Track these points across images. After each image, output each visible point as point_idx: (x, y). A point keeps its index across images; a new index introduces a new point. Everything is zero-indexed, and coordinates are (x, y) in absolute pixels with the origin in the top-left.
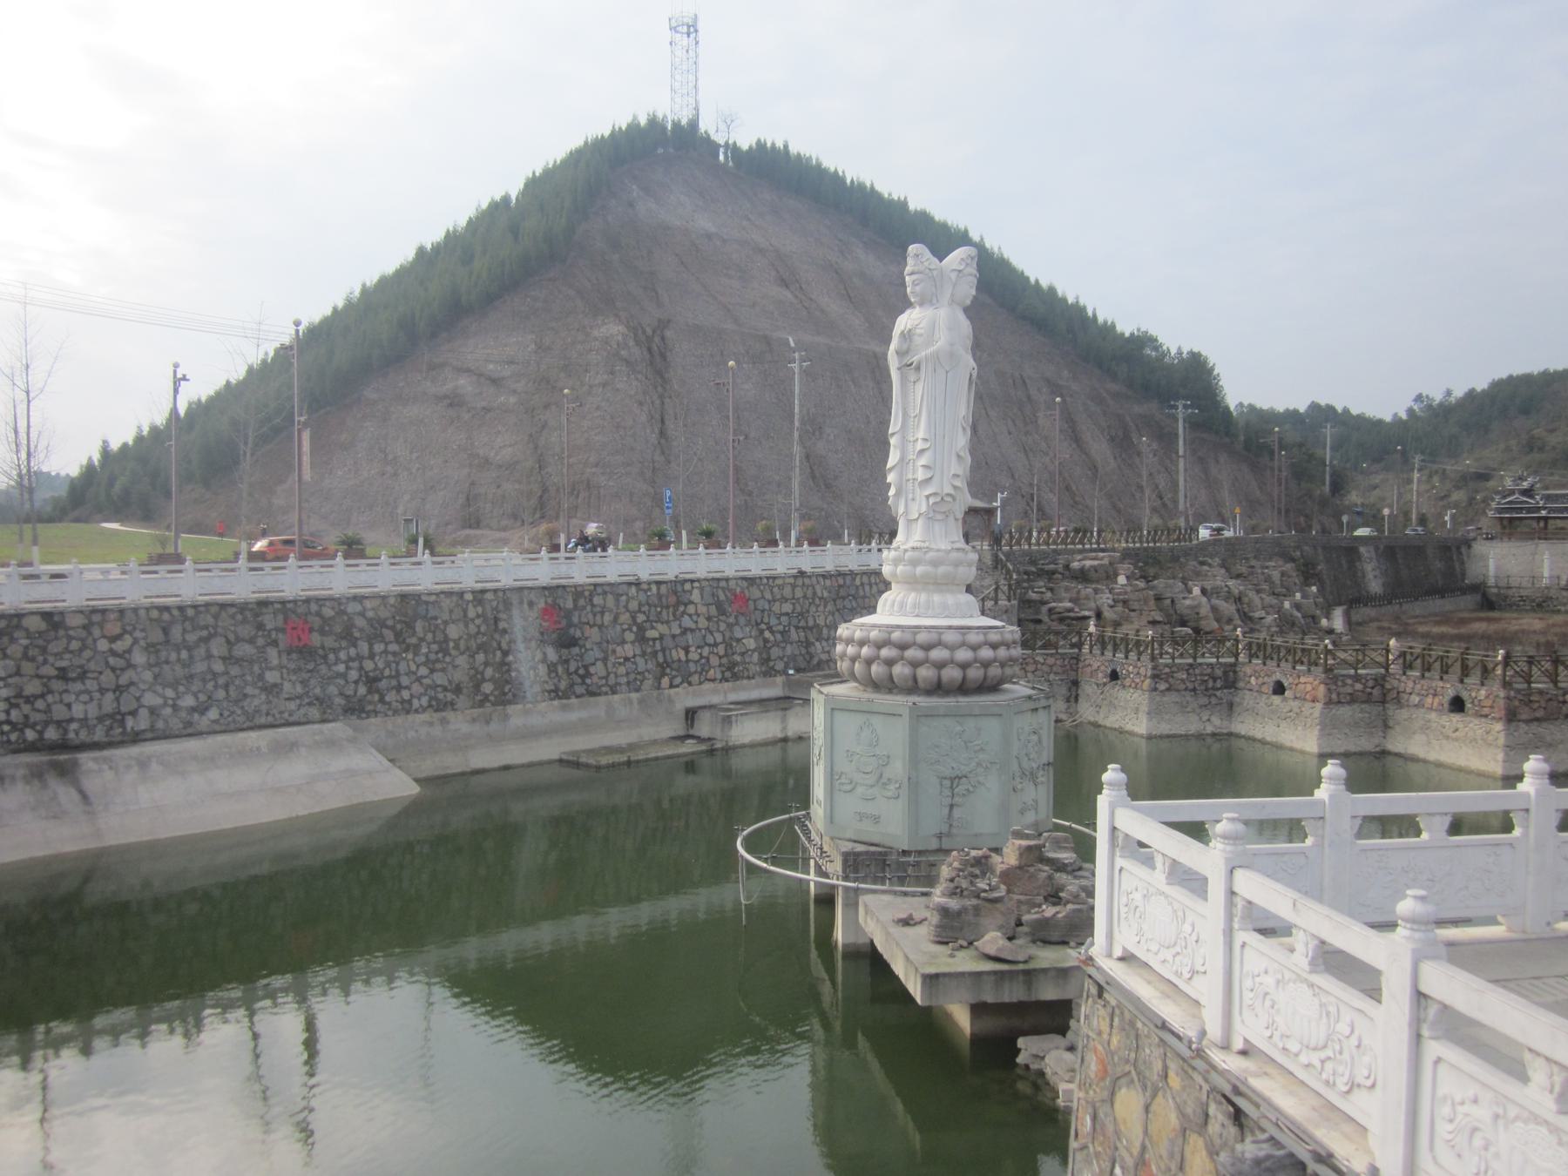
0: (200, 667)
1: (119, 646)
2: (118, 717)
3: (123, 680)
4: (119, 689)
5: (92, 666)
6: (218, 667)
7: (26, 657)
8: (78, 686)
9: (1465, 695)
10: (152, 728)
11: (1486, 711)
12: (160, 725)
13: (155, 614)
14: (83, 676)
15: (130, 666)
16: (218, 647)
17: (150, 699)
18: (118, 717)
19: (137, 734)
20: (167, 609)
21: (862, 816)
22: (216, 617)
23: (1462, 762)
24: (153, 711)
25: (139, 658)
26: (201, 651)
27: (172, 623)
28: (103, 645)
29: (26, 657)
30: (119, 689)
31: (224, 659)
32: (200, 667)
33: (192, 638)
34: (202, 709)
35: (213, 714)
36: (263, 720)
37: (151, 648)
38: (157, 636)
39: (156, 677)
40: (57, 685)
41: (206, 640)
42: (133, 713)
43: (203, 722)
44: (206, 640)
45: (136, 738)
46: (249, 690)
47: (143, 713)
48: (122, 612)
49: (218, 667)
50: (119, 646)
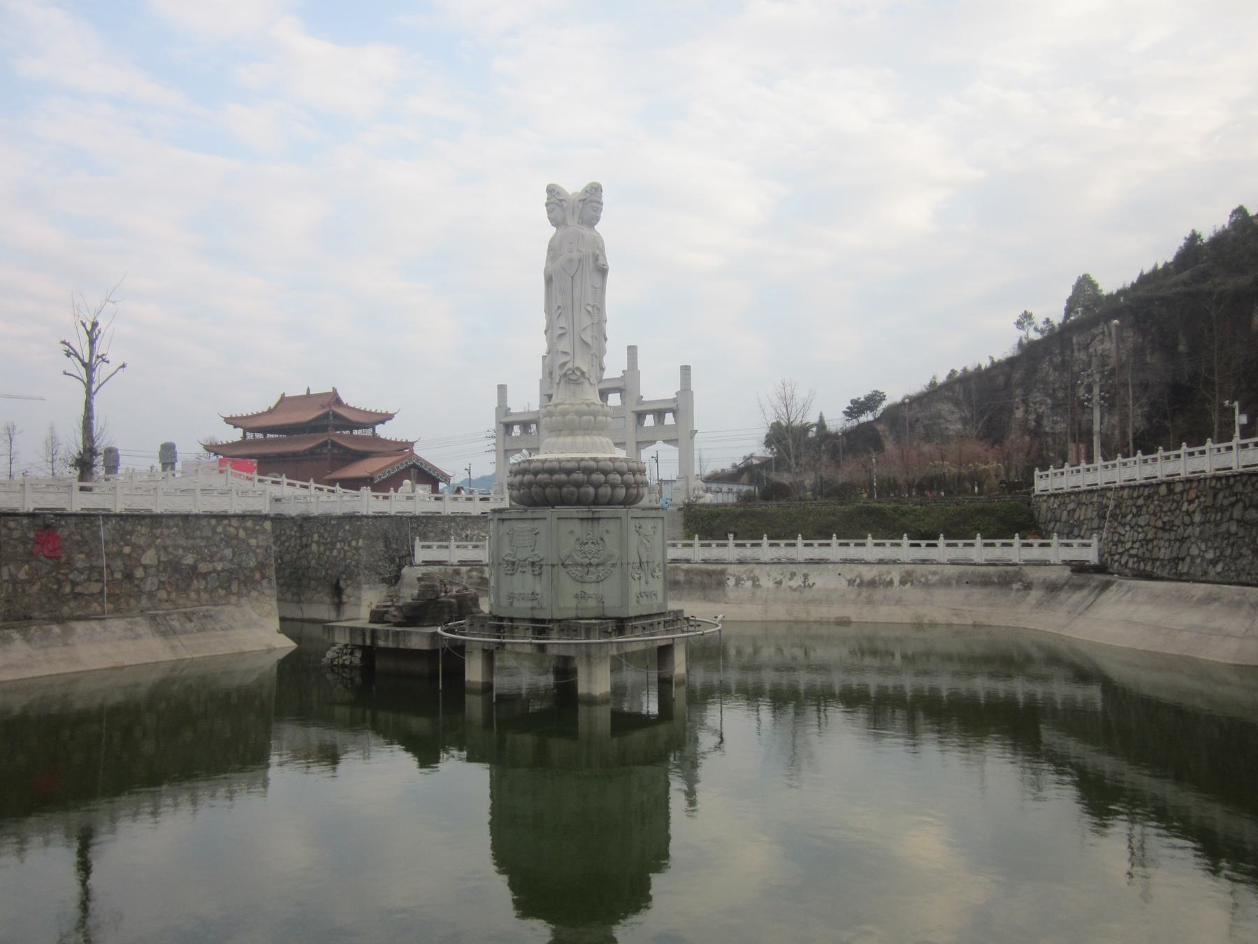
0: (1223, 528)
1: (1192, 507)
2: (1177, 560)
3: (1186, 535)
4: (1183, 540)
5: (1177, 522)
6: (1233, 528)
7: (1154, 514)
8: (1167, 536)
10: (1188, 573)
12: (1192, 571)
13: (1214, 483)
14: (1171, 530)
15: (1192, 523)
16: (1237, 513)
17: (1194, 551)
18: (1177, 560)
19: (1181, 574)
20: (1218, 478)
22: (1244, 485)
24: (1193, 558)
25: (1197, 518)
26: (1228, 514)
27: (1220, 490)
28: (1184, 508)
29: (1154, 514)
30: (1183, 540)
31: (1238, 521)
32: (1223, 528)
33: (1226, 502)
34: (1214, 562)
35: (1219, 568)
36: (1244, 578)
37: (1205, 511)
38: (1209, 502)
39: (1201, 532)
40: (1160, 534)
41: (1233, 505)
42: (1183, 559)
43: (1212, 572)
44: (1233, 505)
45: (1179, 578)
46: (1245, 551)
47: (1188, 559)
48: (1199, 480)
49: (1233, 528)
50: (1192, 507)
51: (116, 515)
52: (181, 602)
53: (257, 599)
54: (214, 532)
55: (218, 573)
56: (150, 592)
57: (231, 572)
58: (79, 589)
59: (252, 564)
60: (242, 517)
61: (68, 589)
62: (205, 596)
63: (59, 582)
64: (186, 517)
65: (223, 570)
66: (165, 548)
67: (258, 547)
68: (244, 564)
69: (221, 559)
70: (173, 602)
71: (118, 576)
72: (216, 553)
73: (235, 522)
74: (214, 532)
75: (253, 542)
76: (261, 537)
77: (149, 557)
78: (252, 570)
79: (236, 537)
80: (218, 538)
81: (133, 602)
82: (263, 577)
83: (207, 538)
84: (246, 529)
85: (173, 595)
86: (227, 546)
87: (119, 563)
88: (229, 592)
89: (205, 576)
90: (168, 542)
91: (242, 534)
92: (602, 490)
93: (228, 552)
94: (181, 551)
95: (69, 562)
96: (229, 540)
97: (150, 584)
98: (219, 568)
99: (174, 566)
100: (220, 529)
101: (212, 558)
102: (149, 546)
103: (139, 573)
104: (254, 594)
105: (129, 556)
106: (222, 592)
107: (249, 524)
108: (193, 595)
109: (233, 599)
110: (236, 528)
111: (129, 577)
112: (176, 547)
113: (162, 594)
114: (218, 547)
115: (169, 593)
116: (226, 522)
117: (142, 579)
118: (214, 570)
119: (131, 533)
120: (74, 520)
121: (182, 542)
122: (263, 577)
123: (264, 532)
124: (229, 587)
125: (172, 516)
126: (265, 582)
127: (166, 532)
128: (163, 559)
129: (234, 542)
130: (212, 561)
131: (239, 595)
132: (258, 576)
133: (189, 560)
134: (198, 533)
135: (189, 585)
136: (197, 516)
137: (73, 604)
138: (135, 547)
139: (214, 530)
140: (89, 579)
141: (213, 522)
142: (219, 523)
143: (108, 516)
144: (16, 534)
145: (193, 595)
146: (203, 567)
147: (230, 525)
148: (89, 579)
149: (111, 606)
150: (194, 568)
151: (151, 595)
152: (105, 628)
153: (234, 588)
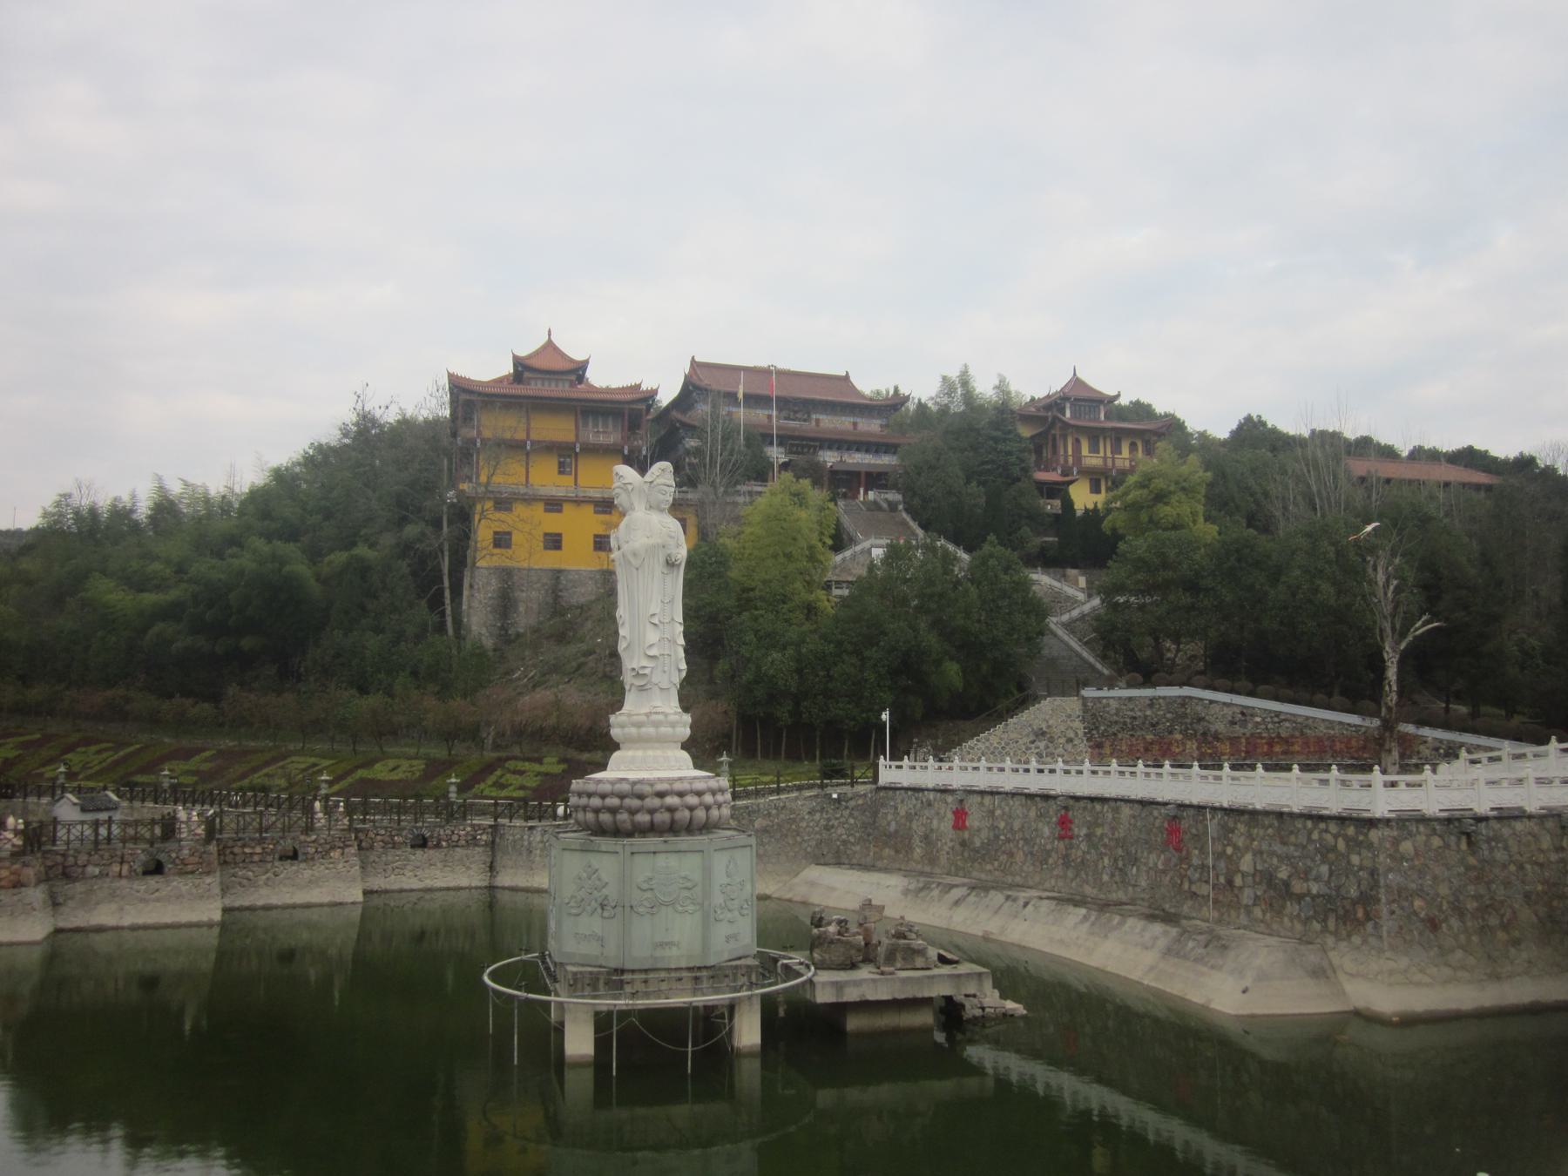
9: (162, 857)
11: (190, 868)
21: (728, 939)
23: (167, 919)
51: (1222, 809)
52: (1275, 926)
53: (1358, 948)
54: (1309, 839)
55: (1314, 898)
56: (1247, 906)
57: (1328, 898)
58: (1194, 888)
59: (1353, 892)
60: (1341, 820)
61: (1186, 886)
62: (1298, 927)
63: (1182, 877)
64: (1280, 815)
65: (1318, 895)
66: (1261, 853)
67: (1361, 868)
68: (1343, 892)
69: (1317, 879)
70: (1268, 926)
71: (1222, 880)
72: (1311, 869)
73: (1333, 828)
74: (1309, 839)
75: (1355, 859)
76: (1365, 852)
77: (1246, 863)
78: (1354, 903)
79: (1334, 849)
80: (1311, 847)
81: (1233, 914)
82: (1368, 917)
83: (1304, 847)
84: (1347, 839)
85: (1268, 915)
86: (1323, 862)
87: (1222, 864)
88: (1325, 929)
89: (1300, 898)
90: (1265, 847)
91: (1341, 845)
92: (678, 815)
93: (1324, 869)
94: (1275, 861)
95: (1188, 858)
96: (1326, 851)
97: (1247, 896)
98: (1314, 891)
99: (1268, 878)
100: (1315, 836)
101: (1305, 875)
102: (1247, 849)
103: (1238, 881)
104: (1356, 940)
105: (1229, 858)
106: (1317, 926)
107: (1351, 831)
108: (1286, 920)
109: (1330, 940)
110: (1336, 837)
111: (1230, 882)
112: (1273, 854)
113: (1258, 912)
114: (1313, 860)
115: (1264, 912)
116: (1322, 826)
117: (1241, 888)
118: (1309, 893)
119: (1232, 831)
120: (1192, 812)
121: (1278, 848)
122: (1368, 917)
123: (1370, 846)
124: (1325, 920)
125: (1266, 813)
126: (1370, 925)
127: (1261, 832)
128: (1259, 868)
129: (1331, 856)
130: (1306, 880)
131: (1336, 933)
132: (1360, 914)
133: (1283, 874)
134: (1292, 839)
135: (1283, 907)
136: (1291, 815)
137: (1190, 903)
138: (1236, 847)
139: (1310, 833)
140: (1200, 880)
141: (1309, 824)
142: (1315, 827)
143: (1214, 809)
144: (1158, 823)
145: (1286, 920)
146: (1298, 887)
147: (1326, 831)
148: (1200, 880)
149: (1216, 915)
150: (1287, 884)
151: (1249, 912)
152: (1143, 930)
153: (1331, 924)
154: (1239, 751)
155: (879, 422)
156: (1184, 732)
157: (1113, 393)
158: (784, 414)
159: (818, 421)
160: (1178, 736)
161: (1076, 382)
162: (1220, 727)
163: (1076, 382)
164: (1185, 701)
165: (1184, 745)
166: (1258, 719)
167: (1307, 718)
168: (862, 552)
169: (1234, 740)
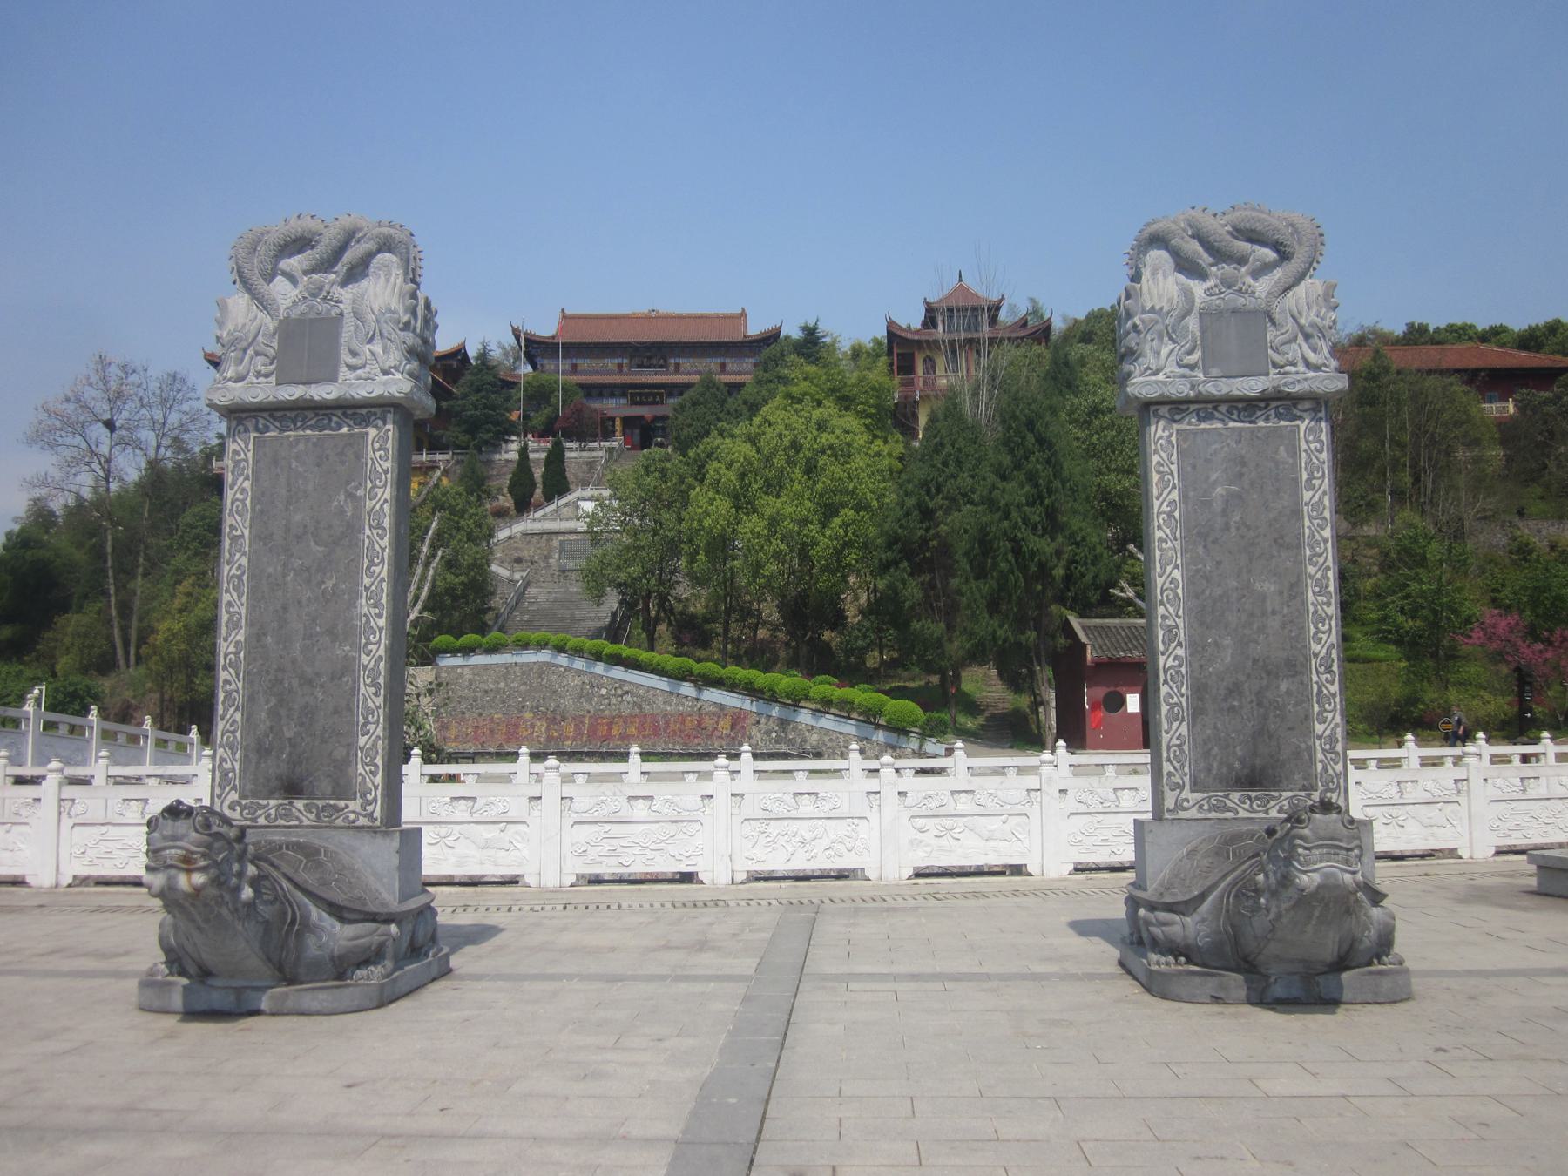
154: (581, 734)
155: (751, 360)
156: (535, 709)
157: (995, 297)
158: (637, 361)
159: (677, 366)
160: (528, 715)
161: (961, 289)
162: (568, 703)
163: (961, 289)
164: (543, 668)
165: (533, 726)
166: (604, 692)
167: (649, 689)
168: (567, 504)
169: (578, 721)
